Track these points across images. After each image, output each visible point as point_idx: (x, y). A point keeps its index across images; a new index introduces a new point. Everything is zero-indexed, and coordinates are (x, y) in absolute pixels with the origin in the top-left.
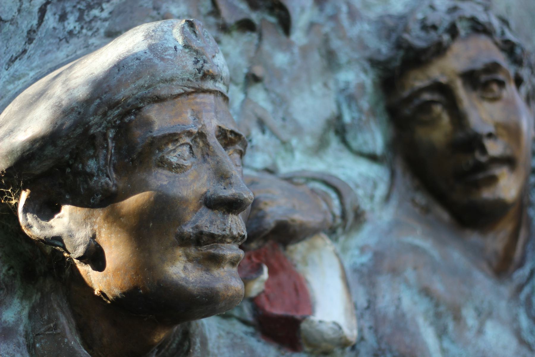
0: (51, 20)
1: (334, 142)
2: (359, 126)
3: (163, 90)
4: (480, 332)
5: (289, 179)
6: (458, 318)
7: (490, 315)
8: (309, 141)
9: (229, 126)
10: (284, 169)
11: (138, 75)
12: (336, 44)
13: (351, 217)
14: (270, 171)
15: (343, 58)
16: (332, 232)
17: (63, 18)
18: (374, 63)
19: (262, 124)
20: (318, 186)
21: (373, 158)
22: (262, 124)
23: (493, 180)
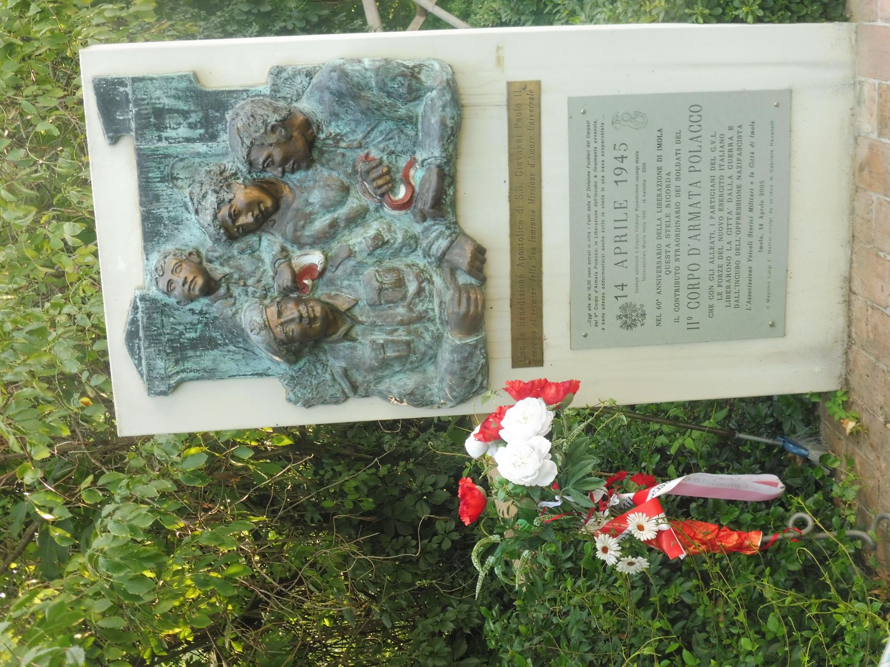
0: (241, 345)
1: (258, 253)
2: (251, 247)
3: (273, 337)
4: (311, 204)
5: (276, 273)
6: (311, 214)
7: (307, 201)
8: (260, 264)
9: (276, 316)
10: (271, 273)
11: (270, 346)
12: (225, 257)
13: (284, 254)
14: (274, 278)
15: (230, 255)
16: (290, 260)
17: (239, 342)
18: (231, 244)
19: (259, 281)
20: (276, 265)
21: (260, 240)
22: (259, 281)
23: (266, 208)
